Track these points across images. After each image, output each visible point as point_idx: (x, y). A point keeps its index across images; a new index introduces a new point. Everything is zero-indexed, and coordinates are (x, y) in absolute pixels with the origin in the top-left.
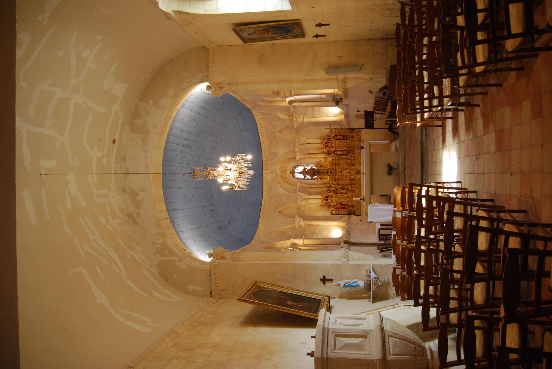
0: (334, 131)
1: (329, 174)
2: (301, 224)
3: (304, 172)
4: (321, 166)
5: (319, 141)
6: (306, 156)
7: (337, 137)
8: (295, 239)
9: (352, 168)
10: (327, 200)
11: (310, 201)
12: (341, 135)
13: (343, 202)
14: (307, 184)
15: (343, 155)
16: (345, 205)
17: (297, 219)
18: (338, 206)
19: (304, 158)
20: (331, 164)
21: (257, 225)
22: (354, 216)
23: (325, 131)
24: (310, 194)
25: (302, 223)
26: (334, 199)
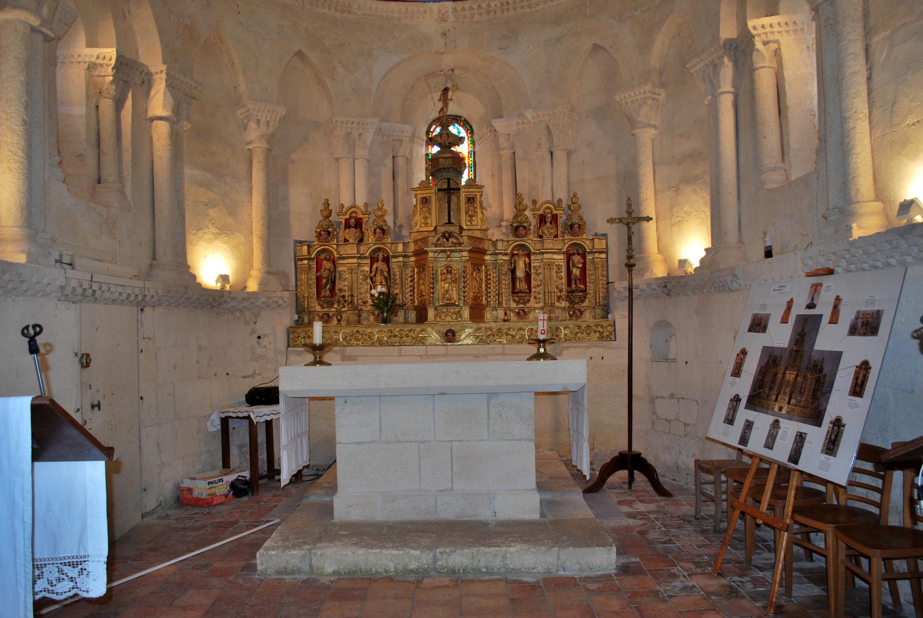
0: (599, 244)
1: (442, 229)
2: (252, 125)
4: (471, 200)
6: (506, 154)
7: (577, 259)
9: (466, 313)
10: (347, 225)
11: (345, 165)
12: (584, 270)
13: (339, 284)
15: (514, 279)
16: (332, 290)
18: (327, 265)
19: (498, 148)
20: (477, 234)
23: (599, 215)
24: (372, 173)
25: (254, 134)
26: (351, 250)
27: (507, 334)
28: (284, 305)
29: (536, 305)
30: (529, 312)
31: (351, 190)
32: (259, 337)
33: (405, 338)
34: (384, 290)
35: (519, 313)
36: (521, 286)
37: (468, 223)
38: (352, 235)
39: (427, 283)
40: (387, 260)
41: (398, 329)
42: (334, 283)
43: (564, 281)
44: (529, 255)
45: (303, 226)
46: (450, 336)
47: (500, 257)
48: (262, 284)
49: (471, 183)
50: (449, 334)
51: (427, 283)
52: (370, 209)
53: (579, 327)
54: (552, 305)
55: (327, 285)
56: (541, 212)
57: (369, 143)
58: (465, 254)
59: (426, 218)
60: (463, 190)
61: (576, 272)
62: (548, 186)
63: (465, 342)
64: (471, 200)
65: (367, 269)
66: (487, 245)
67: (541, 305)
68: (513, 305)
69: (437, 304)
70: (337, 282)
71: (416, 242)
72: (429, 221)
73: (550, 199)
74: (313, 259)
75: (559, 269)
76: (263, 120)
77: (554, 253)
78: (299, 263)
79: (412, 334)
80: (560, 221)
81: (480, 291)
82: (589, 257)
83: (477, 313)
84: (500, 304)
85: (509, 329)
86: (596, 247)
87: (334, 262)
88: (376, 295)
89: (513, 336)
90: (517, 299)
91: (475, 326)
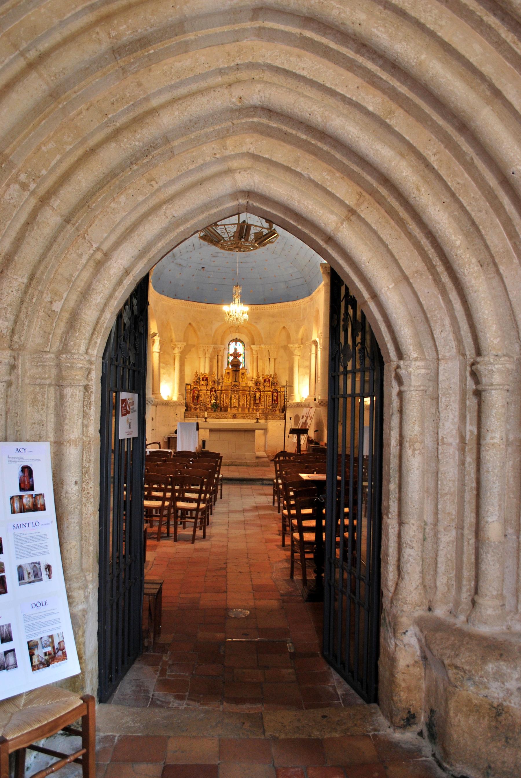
1: (233, 383)
2: (176, 349)
3: (236, 355)
4: (243, 374)
5: (272, 373)
6: (255, 357)
7: (275, 394)
8: (160, 343)
9: (240, 409)
10: (203, 380)
11: (202, 360)
12: (277, 397)
13: (200, 399)
14: (222, 357)
15: (255, 400)
16: (197, 400)
17: (181, 345)
19: (253, 354)
20: (244, 385)
21: (176, 297)
22: (184, 410)
23: (283, 381)
24: (211, 360)
31: (204, 368)
45: (189, 379)
48: (178, 398)
49: (243, 368)
55: (196, 398)
62: (268, 370)
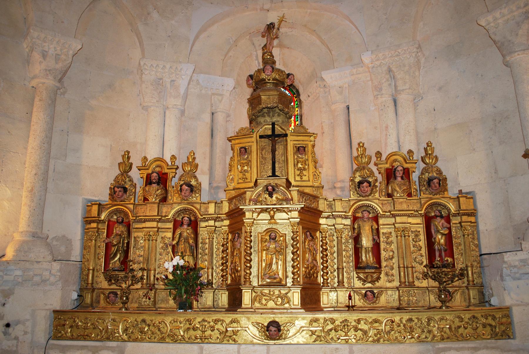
9: (296, 297)
12: (449, 237)
15: (357, 250)
27: (356, 329)
28: (52, 279)
29: (389, 285)
30: (380, 293)
31: (158, 139)
32: (8, 325)
33: (208, 332)
34: (182, 263)
35: (365, 295)
36: (367, 257)
37: (298, 178)
38: (155, 190)
39: (243, 254)
40: (194, 225)
41: (199, 319)
42: (126, 252)
43: (424, 251)
44: (376, 219)
46: (273, 331)
47: (339, 220)
50: (273, 329)
51: (243, 254)
52: (178, 163)
53: (461, 320)
54: (411, 285)
56: (388, 166)
57: (182, 91)
58: (295, 214)
59: (243, 172)
60: (289, 138)
61: (440, 239)
63: (295, 341)
64: (300, 150)
65: (169, 235)
66: (322, 205)
67: (396, 283)
68: (358, 284)
69: (255, 284)
70: (132, 250)
71: (230, 200)
72: (248, 175)
73: (395, 149)
74: (103, 222)
75: (417, 236)
76: (51, 52)
77: (409, 216)
78: (88, 226)
79: (218, 326)
80: (415, 177)
81: (315, 267)
82: (455, 221)
83: (311, 301)
84: (341, 283)
85: (358, 321)
86: (463, 207)
87: (128, 226)
88: (171, 270)
89: (365, 332)
90: (361, 276)
91: (310, 316)
